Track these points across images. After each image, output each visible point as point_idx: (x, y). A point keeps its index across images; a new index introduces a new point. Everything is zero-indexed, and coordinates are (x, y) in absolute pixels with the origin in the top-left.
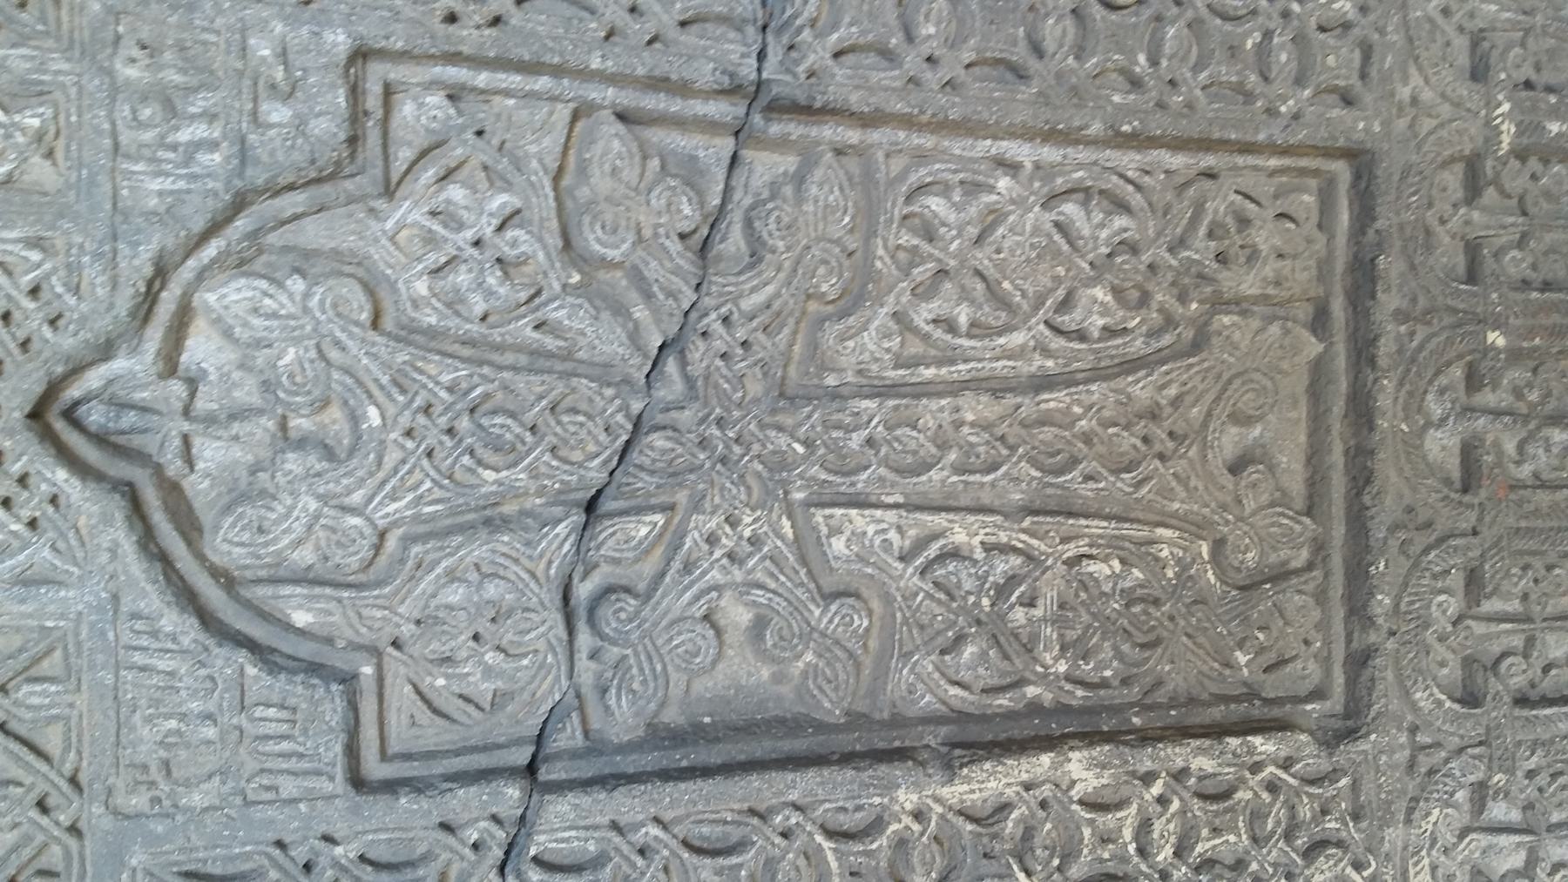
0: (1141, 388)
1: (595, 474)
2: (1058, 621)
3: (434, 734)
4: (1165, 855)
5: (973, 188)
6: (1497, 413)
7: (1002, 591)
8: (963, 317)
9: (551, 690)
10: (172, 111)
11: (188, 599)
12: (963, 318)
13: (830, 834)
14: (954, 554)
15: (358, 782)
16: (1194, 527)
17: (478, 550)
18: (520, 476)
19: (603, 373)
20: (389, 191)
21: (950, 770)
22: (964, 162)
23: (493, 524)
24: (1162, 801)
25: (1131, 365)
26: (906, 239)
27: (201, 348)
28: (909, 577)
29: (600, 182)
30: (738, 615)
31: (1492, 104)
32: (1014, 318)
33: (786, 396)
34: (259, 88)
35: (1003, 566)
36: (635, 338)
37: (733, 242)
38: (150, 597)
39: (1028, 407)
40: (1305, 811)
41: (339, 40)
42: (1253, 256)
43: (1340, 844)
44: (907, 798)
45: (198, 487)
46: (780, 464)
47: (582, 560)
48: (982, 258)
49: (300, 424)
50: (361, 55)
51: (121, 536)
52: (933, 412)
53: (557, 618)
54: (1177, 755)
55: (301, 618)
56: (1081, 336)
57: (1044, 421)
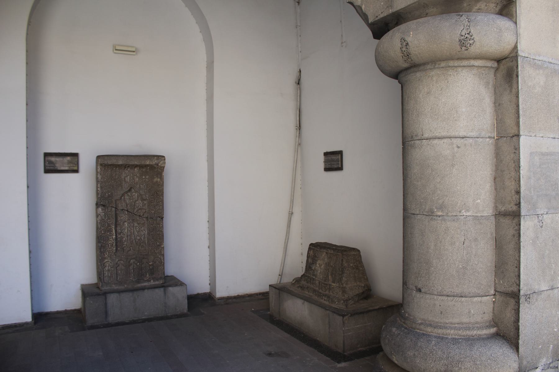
0: (134, 241)
1: (129, 211)
2: (122, 237)
3: (117, 203)
4: (109, 242)
5: (144, 230)
6: (134, 265)
7: (123, 233)
8: (137, 230)
9: (119, 209)
10: (144, 192)
11: (124, 193)
12: (137, 230)
13: (112, 222)
14: (125, 230)
15: (116, 200)
16: (126, 245)
17: (125, 205)
18: (129, 207)
19: (134, 211)
20: (141, 201)
21: (115, 229)
22: (145, 229)
23: (127, 206)
24: (112, 242)
25: (135, 240)
26: (141, 226)
27: (134, 193)
28: (124, 227)
29: (143, 210)
30: (122, 218)
31: (152, 262)
32: (137, 233)
33: (133, 220)
34: (145, 195)
35: (124, 233)
36: (135, 213)
37: (140, 217)
38: (124, 192)
39: (133, 234)
40: (111, 252)
41: (148, 198)
42: (142, 248)
43: (109, 254)
44: (113, 227)
45: (128, 193)
46: (130, 220)
47: (125, 210)
48: (140, 231)
49: (131, 198)
50: (147, 199)
51: (127, 190)
52: (132, 229)
53: (122, 209)
54: (115, 243)
55: (122, 198)
56: (137, 237)
57: (132, 235)
